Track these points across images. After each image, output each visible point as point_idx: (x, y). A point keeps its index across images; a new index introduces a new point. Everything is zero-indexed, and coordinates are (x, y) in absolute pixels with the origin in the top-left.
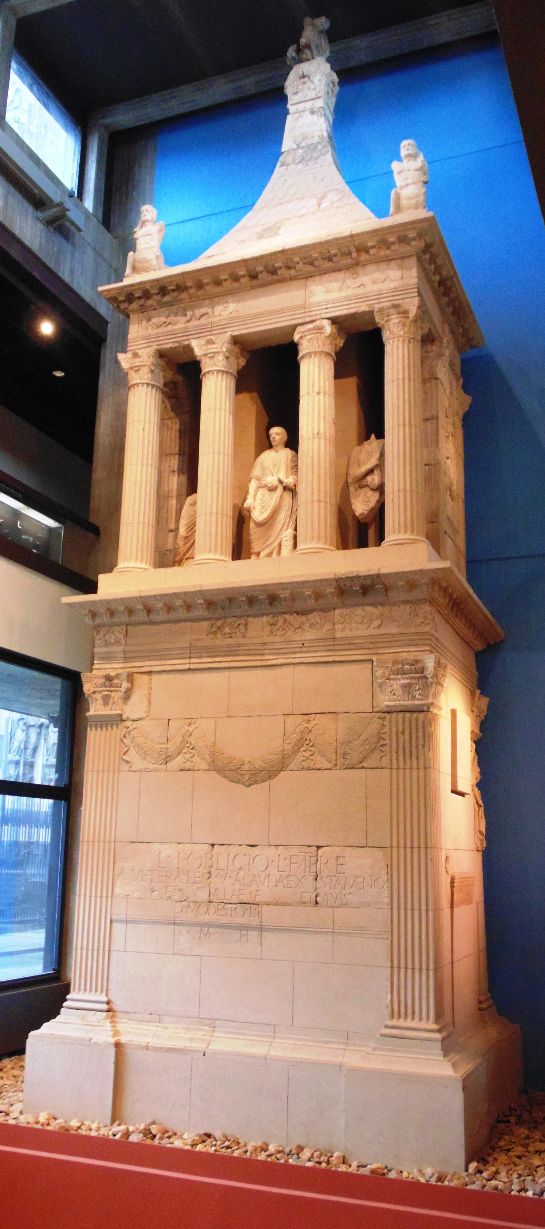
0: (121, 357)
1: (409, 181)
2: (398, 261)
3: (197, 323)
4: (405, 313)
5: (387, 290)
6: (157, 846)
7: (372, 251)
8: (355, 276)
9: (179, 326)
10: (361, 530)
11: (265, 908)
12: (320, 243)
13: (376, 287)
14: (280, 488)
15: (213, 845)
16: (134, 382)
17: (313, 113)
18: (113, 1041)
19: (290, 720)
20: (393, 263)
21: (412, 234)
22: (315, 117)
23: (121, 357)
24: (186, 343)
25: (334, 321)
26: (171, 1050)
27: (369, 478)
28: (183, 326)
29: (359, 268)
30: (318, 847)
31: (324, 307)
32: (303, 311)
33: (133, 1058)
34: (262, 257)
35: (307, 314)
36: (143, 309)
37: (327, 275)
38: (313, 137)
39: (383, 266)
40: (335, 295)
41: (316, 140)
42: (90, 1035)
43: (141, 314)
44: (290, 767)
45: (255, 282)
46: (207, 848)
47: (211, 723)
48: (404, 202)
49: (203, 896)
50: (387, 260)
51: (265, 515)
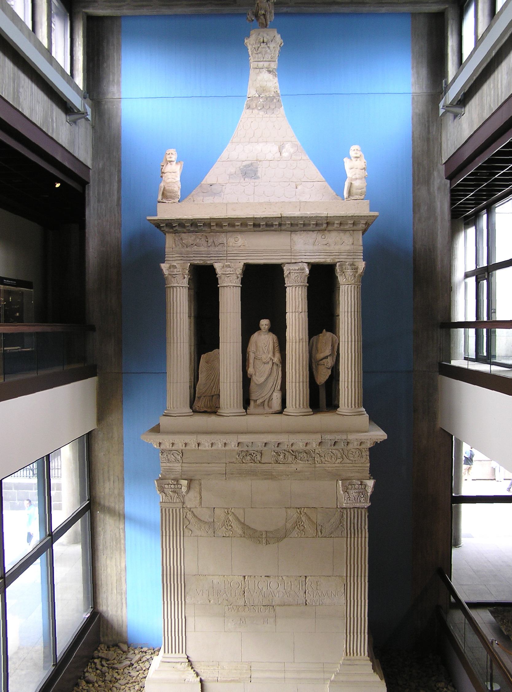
0: (162, 265)
1: (358, 176)
2: (351, 232)
3: (217, 249)
4: (356, 269)
5: (344, 252)
6: (211, 577)
7: (336, 225)
8: (323, 237)
9: (202, 249)
10: (322, 396)
11: (277, 608)
13: (337, 247)
14: (271, 363)
16: (172, 285)
17: (269, 72)
18: (198, 679)
19: (289, 510)
20: (348, 234)
22: (270, 76)
23: (162, 265)
24: (209, 262)
25: (308, 263)
28: (206, 249)
29: (326, 232)
31: (304, 254)
32: (290, 254)
33: (208, 685)
35: (293, 257)
36: (175, 232)
38: (270, 91)
39: (342, 234)
40: (310, 247)
42: (183, 677)
43: (174, 235)
44: (290, 536)
46: (242, 578)
47: (241, 511)
48: (354, 190)
50: (345, 231)
51: (262, 380)
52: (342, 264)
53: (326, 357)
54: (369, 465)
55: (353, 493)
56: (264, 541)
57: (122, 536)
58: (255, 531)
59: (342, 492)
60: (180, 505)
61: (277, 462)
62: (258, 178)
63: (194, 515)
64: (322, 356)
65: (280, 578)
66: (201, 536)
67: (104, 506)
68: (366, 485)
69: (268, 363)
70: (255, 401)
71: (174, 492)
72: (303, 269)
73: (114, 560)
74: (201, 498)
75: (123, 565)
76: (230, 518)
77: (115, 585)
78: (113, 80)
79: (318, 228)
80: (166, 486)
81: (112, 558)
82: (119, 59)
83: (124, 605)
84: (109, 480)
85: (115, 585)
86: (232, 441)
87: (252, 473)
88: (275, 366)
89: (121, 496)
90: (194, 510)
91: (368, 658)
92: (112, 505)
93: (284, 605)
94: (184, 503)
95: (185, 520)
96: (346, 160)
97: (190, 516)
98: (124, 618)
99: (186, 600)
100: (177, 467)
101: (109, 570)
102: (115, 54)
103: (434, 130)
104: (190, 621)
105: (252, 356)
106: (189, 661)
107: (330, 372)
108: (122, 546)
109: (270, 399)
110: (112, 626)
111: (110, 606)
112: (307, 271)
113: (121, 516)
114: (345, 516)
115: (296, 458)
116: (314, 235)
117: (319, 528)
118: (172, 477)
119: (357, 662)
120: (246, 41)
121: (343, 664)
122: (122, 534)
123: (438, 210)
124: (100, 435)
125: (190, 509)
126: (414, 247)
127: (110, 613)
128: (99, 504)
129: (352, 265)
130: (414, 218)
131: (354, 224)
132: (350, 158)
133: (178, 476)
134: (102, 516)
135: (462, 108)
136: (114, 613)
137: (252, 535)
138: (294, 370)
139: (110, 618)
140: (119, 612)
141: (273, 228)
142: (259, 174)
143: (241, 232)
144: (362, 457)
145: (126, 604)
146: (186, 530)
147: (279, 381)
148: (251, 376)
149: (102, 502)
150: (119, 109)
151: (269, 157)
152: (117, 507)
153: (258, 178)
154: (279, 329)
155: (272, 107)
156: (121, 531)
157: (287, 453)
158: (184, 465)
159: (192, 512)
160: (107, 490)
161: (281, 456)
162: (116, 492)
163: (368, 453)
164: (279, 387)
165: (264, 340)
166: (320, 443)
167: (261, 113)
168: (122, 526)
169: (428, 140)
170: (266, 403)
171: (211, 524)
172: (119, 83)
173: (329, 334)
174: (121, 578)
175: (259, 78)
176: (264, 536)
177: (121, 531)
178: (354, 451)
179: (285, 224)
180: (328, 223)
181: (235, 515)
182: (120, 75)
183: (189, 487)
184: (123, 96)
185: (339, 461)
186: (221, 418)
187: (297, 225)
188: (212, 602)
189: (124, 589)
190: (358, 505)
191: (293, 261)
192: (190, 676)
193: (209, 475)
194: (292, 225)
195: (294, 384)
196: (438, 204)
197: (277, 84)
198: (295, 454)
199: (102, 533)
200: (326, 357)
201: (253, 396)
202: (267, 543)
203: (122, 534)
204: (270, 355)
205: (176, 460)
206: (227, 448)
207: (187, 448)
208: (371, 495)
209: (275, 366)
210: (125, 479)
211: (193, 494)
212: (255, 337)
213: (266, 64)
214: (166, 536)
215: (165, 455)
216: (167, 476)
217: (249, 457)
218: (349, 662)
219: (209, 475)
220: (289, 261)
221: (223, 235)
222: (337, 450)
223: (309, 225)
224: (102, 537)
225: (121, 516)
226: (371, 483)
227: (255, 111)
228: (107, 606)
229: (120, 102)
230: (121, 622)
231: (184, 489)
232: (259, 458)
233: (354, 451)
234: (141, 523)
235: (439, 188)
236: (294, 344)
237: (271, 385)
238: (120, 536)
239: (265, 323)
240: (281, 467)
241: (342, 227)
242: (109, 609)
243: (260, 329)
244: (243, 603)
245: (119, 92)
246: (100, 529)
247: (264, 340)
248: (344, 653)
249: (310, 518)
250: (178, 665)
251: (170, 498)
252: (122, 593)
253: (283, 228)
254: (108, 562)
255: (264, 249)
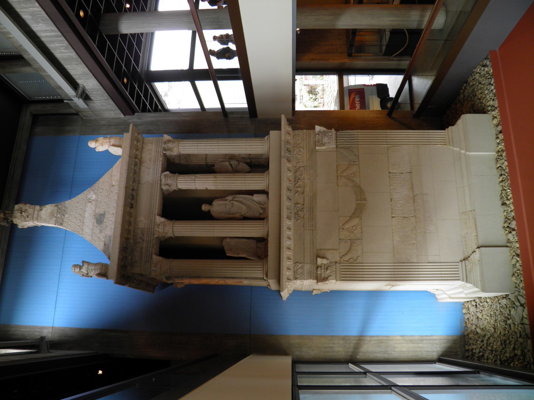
3: (145, 236)
4: (169, 141)
7: (137, 153)
12: (128, 170)
15: (392, 217)
17: (41, 210)
18: (477, 250)
20: (145, 146)
21: (136, 135)
24: (154, 241)
25: (162, 172)
26: (476, 225)
27: (233, 166)
30: (390, 173)
34: (125, 197)
37: (141, 174)
39: (144, 150)
41: (56, 208)
45: (134, 206)
48: (117, 143)
49: (413, 220)
51: (244, 207)
52: (165, 149)
53: (231, 165)
54: (305, 130)
55: (326, 140)
56: (363, 202)
57: (376, 338)
58: (356, 209)
59: (324, 148)
60: (338, 265)
61: (303, 193)
62: (105, 212)
63: (345, 255)
64: (230, 167)
65: (392, 191)
66: (362, 250)
67: (353, 352)
68: (319, 132)
69: (233, 204)
70: (261, 214)
71: (327, 269)
72: (165, 175)
73: (396, 345)
74: (332, 249)
75: (399, 338)
76: (347, 227)
77: (415, 345)
78: (39, 332)
79: (138, 165)
80: (323, 276)
81: (394, 347)
82: (26, 327)
83: (431, 338)
84: (332, 347)
85: (415, 345)
86: (286, 223)
87: (312, 210)
88: (235, 199)
89: (345, 338)
90: (342, 254)
91: (447, 129)
92: (352, 345)
93: (413, 188)
94: (336, 262)
95: (349, 261)
96: (97, 150)
97: (346, 258)
98: (443, 338)
99: (415, 261)
100: (307, 267)
101: (404, 350)
102: (22, 330)
103: (103, 123)
104: (431, 259)
105: (227, 216)
106: (464, 260)
107: (241, 163)
108: (384, 338)
109: (259, 203)
110: (449, 348)
111: (434, 349)
112: (167, 173)
113: (360, 339)
114: (343, 146)
115: (299, 179)
116: (143, 168)
117: (352, 163)
118: (315, 271)
119: (450, 137)
120: (20, 227)
121: (453, 146)
122: (375, 338)
123: (153, 119)
124: (297, 353)
125: (341, 258)
126: (174, 133)
127: (439, 349)
128: (351, 356)
129: (165, 143)
130: (156, 133)
131: (138, 141)
132: (95, 148)
133: (315, 266)
134: (361, 354)
135: (79, 87)
136: (438, 346)
137: (359, 211)
138: (236, 182)
139: (443, 350)
140: (437, 342)
141: (135, 195)
142: (102, 212)
143: (136, 218)
144: (299, 135)
145: (430, 336)
146: (358, 261)
147: (246, 196)
148: (241, 215)
149: (350, 354)
150: (60, 329)
151: (93, 207)
152: (353, 342)
153: (105, 212)
154: (210, 197)
155: (64, 208)
156: (372, 339)
157: (297, 185)
158: (306, 262)
159: (343, 256)
160: (341, 349)
161: (299, 189)
162: (342, 342)
163: (296, 131)
164: (250, 196)
165: (217, 207)
166: (289, 161)
167: (66, 216)
168: (368, 338)
169: (109, 125)
170: (262, 206)
171: (352, 242)
172: (42, 328)
173: (216, 166)
174: (409, 340)
175: (44, 217)
176: (359, 202)
177: (372, 339)
178: (295, 140)
179: (133, 186)
180: (135, 158)
181: (344, 224)
182: (37, 327)
183: (323, 258)
184: (51, 325)
185: (302, 150)
186: (270, 232)
187: (134, 179)
188: (414, 242)
189: (418, 338)
190: (334, 137)
191: (159, 182)
192: (476, 256)
193: (313, 242)
194: (134, 182)
195: (246, 182)
196: (149, 119)
197: (50, 205)
198: (296, 180)
199: (374, 355)
200: (231, 165)
201: (257, 215)
202: (365, 200)
203: (375, 338)
204: (227, 202)
205: (302, 268)
206: (292, 228)
207: (292, 257)
208: (327, 129)
209: (235, 199)
210: (331, 334)
211: (329, 254)
212: (214, 214)
213: (36, 212)
214: (363, 277)
215: (299, 276)
216: (315, 275)
217: (300, 213)
218: (451, 142)
219: (313, 242)
220: (159, 185)
221: (136, 231)
222: (294, 151)
223: (135, 170)
224: (378, 355)
225: (360, 339)
226: (318, 128)
227: (65, 220)
228: (433, 351)
229: (55, 327)
230: (445, 341)
231: (325, 261)
232: (299, 206)
233: (295, 140)
234: (366, 323)
235: (140, 119)
236: (217, 182)
237: (249, 202)
238: (376, 340)
239: (205, 208)
240: (307, 189)
241: (139, 149)
242: (435, 350)
243: (209, 211)
244: (414, 218)
245: (47, 328)
246: (372, 356)
247: (217, 207)
248: (445, 146)
249: (345, 170)
250: (468, 268)
251: (332, 273)
252: (422, 339)
253: (135, 188)
254: (397, 350)
255: (150, 203)
